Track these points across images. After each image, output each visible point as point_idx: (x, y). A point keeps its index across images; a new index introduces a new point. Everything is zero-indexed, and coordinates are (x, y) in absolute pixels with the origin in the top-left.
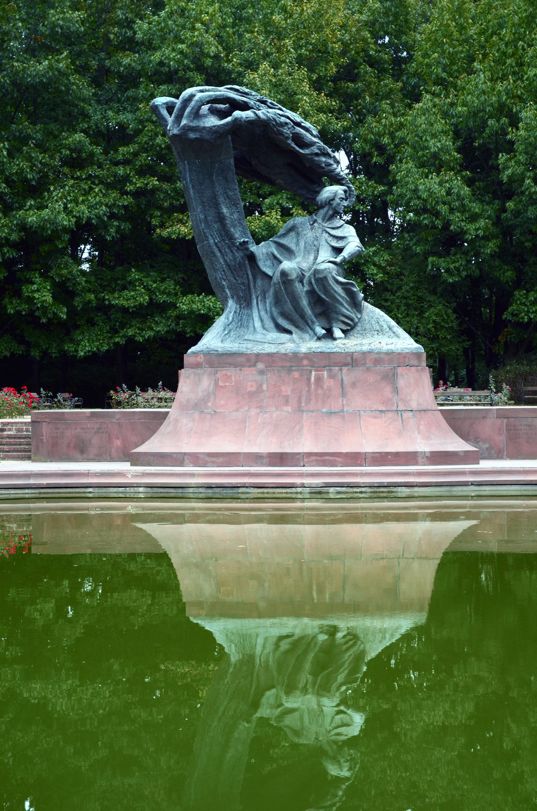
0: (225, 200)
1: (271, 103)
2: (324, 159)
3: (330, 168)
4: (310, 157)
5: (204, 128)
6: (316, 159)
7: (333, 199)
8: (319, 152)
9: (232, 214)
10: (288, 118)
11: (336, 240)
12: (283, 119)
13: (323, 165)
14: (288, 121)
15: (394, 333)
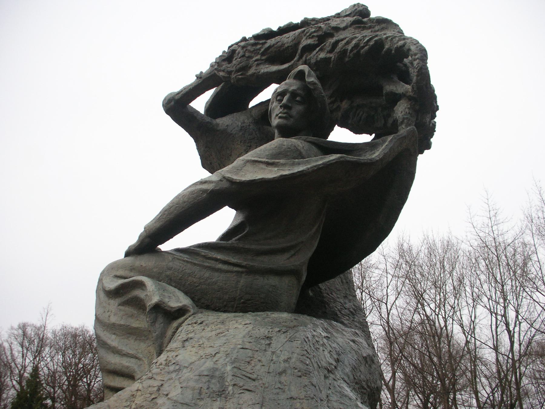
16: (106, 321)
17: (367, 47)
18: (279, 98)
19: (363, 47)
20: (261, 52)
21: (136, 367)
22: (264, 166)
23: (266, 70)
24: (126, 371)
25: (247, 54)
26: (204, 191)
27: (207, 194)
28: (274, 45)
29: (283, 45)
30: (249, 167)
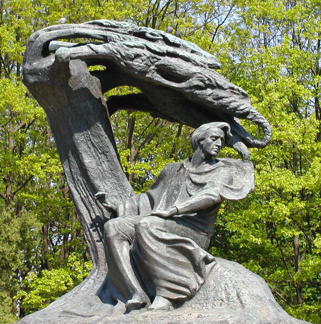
0: (89, 148)
1: (151, 34)
2: (209, 91)
3: (221, 101)
4: (188, 91)
5: (41, 70)
6: (197, 92)
7: (202, 139)
8: (201, 84)
9: (99, 164)
10: (149, 49)
11: (196, 188)
12: (132, 52)
13: (210, 99)
14: (145, 52)
15: (241, 303)
16: (163, 254)
17: (242, 112)
18: (214, 138)
19: (238, 110)
20: (156, 64)
21: (189, 282)
22: (229, 190)
23: (159, 80)
24: (183, 283)
25: (149, 63)
26: (213, 201)
27: (214, 202)
28: (168, 65)
29: (175, 70)
30: (225, 190)
